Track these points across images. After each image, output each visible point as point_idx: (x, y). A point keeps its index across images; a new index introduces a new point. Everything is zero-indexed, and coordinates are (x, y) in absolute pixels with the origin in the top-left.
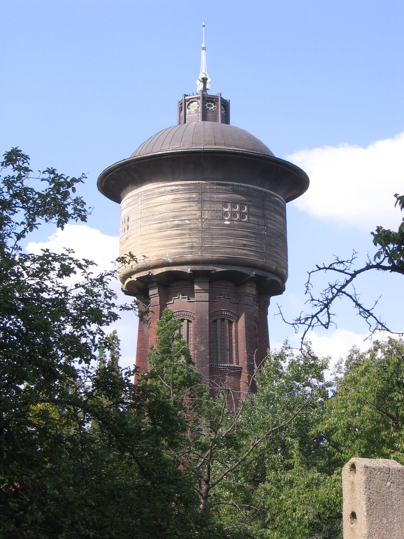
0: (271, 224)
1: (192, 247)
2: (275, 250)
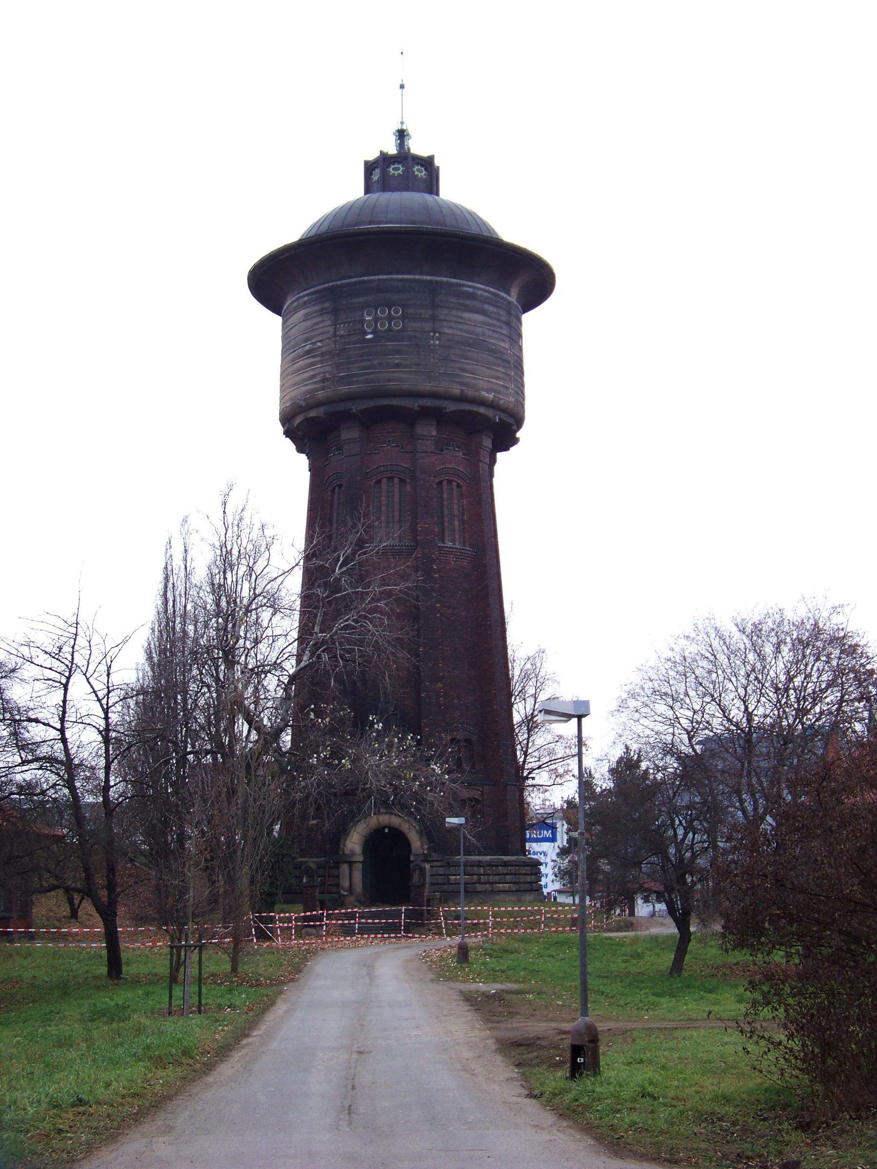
0: (449, 327)
1: (324, 380)
2: (457, 365)
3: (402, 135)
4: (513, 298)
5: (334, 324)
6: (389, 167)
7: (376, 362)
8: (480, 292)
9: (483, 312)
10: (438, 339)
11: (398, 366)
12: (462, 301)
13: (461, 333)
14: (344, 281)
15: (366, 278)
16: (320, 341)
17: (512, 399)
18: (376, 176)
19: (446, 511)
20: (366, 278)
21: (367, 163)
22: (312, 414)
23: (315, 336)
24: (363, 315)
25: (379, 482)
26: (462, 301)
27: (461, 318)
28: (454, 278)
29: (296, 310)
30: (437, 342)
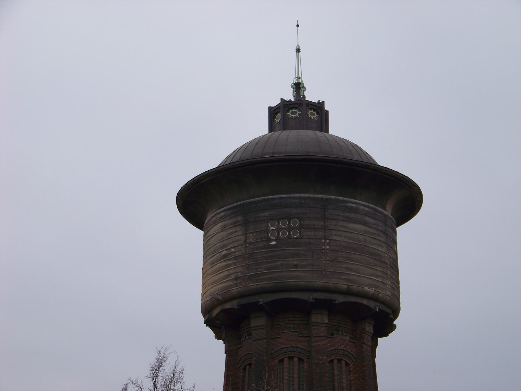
1: (236, 279)
3: (298, 87)
4: (388, 213)
5: (245, 234)
6: (288, 111)
7: (278, 263)
8: (362, 207)
9: (364, 223)
10: (328, 244)
11: (296, 266)
12: (347, 214)
13: (346, 240)
14: (252, 200)
15: (270, 197)
16: (233, 248)
17: (389, 293)
18: (278, 118)
19: (336, 384)
20: (270, 197)
21: (270, 108)
22: (228, 306)
23: (229, 244)
24: (268, 226)
25: (282, 361)
26: (347, 214)
27: (347, 227)
28: (339, 196)
29: (215, 223)
30: (328, 247)
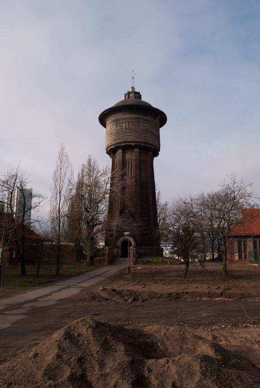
1: (114, 139)
4: (157, 121)
5: (116, 127)
22: (111, 147)
